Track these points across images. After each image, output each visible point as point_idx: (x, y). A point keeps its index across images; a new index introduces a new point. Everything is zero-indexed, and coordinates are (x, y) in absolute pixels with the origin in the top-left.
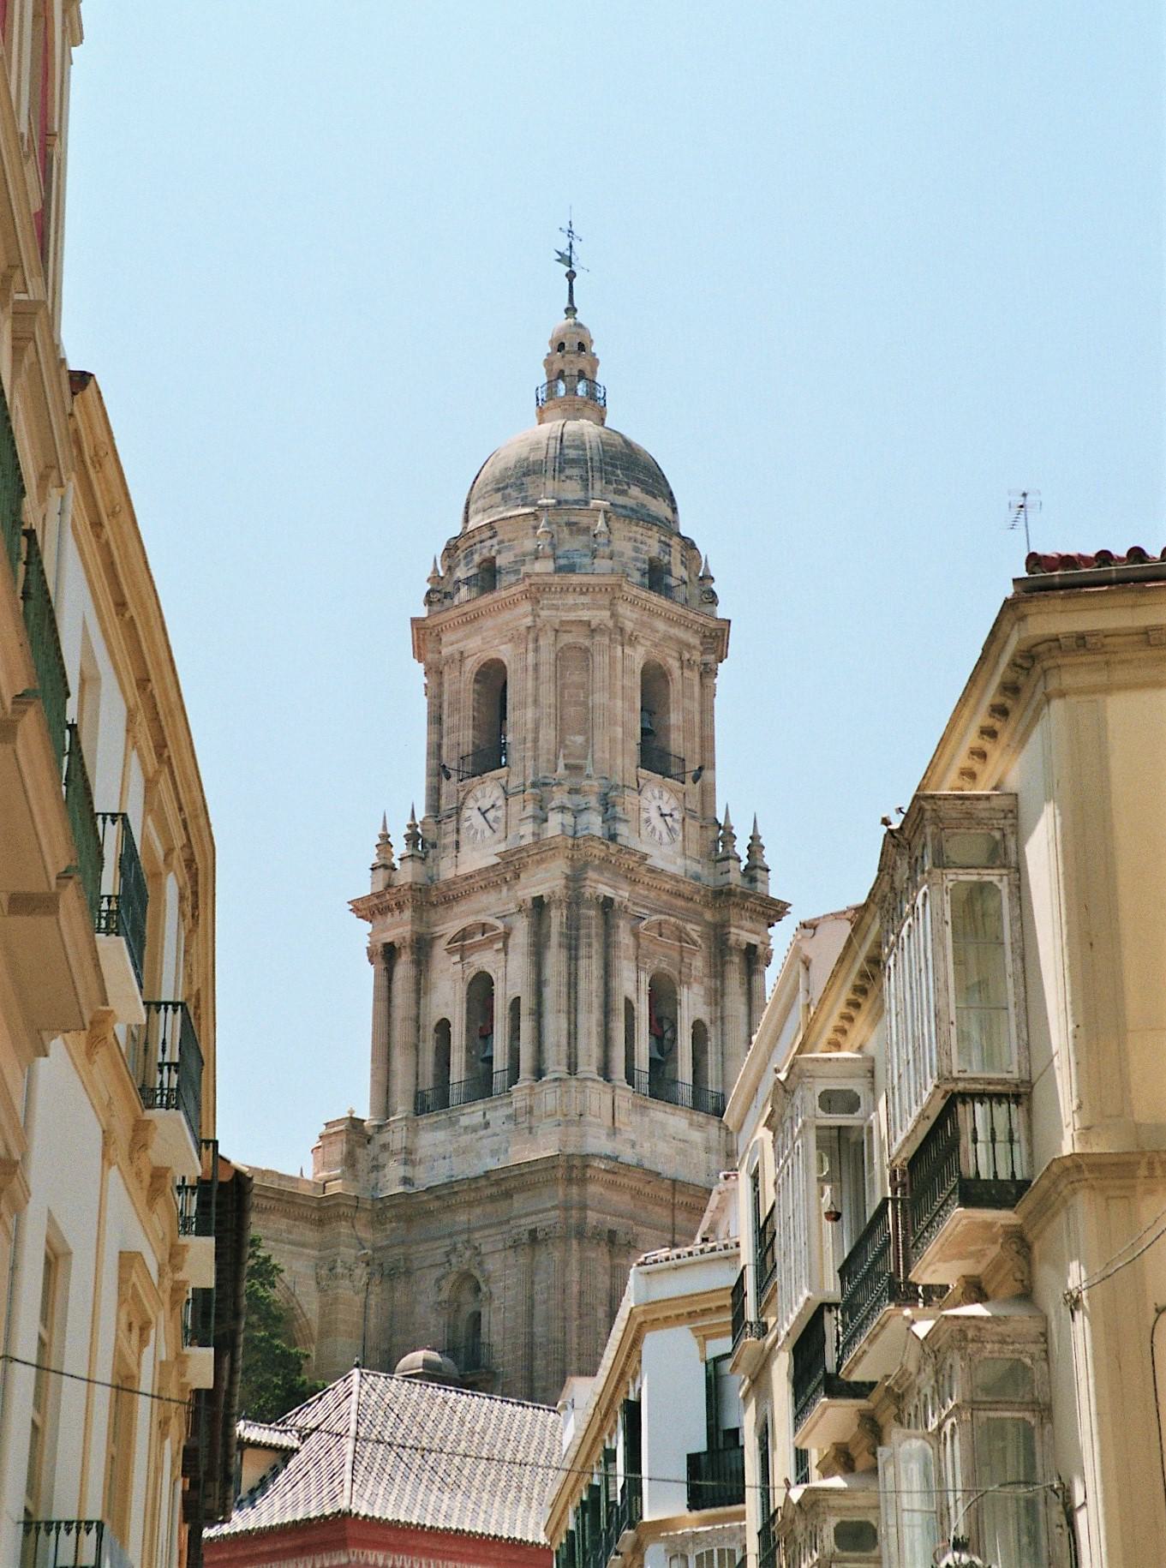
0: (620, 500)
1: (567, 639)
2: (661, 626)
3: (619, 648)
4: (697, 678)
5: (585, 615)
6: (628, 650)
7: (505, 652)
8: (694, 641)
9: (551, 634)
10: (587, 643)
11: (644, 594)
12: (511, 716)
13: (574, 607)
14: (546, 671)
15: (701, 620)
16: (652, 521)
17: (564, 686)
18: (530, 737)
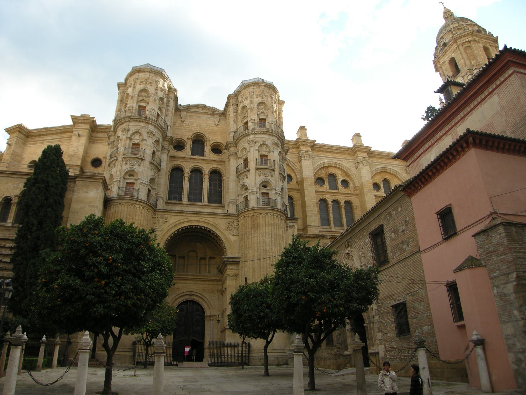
0: (467, 24)
1: (465, 46)
2: (483, 40)
3: (477, 44)
4: (495, 49)
5: (467, 40)
6: (479, 44)
7: (453, 55)
8: (492, 42)
9: (461, 46)
10: (469, 45)
11: (478, 34)
12: (458, 64)
13: (465, 40)
14: (463, 51)
15: (492, 38)
16: (474, 25)
17: (467, 54)
18: (464, 64)
